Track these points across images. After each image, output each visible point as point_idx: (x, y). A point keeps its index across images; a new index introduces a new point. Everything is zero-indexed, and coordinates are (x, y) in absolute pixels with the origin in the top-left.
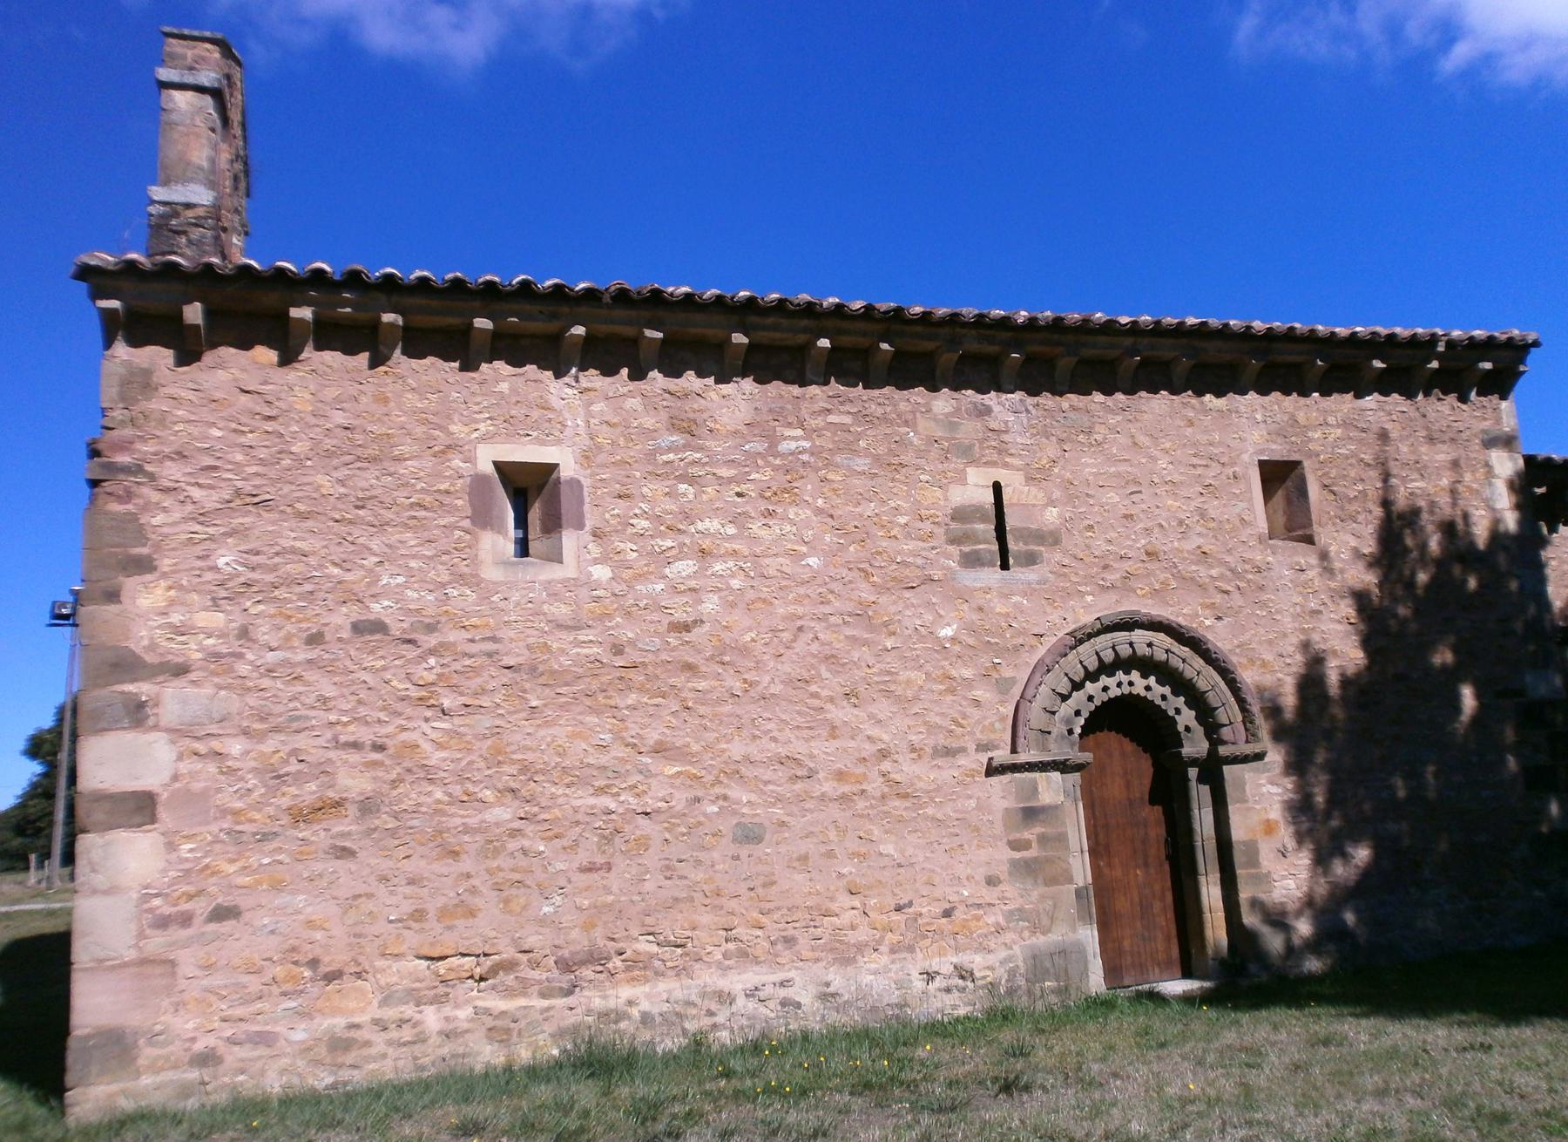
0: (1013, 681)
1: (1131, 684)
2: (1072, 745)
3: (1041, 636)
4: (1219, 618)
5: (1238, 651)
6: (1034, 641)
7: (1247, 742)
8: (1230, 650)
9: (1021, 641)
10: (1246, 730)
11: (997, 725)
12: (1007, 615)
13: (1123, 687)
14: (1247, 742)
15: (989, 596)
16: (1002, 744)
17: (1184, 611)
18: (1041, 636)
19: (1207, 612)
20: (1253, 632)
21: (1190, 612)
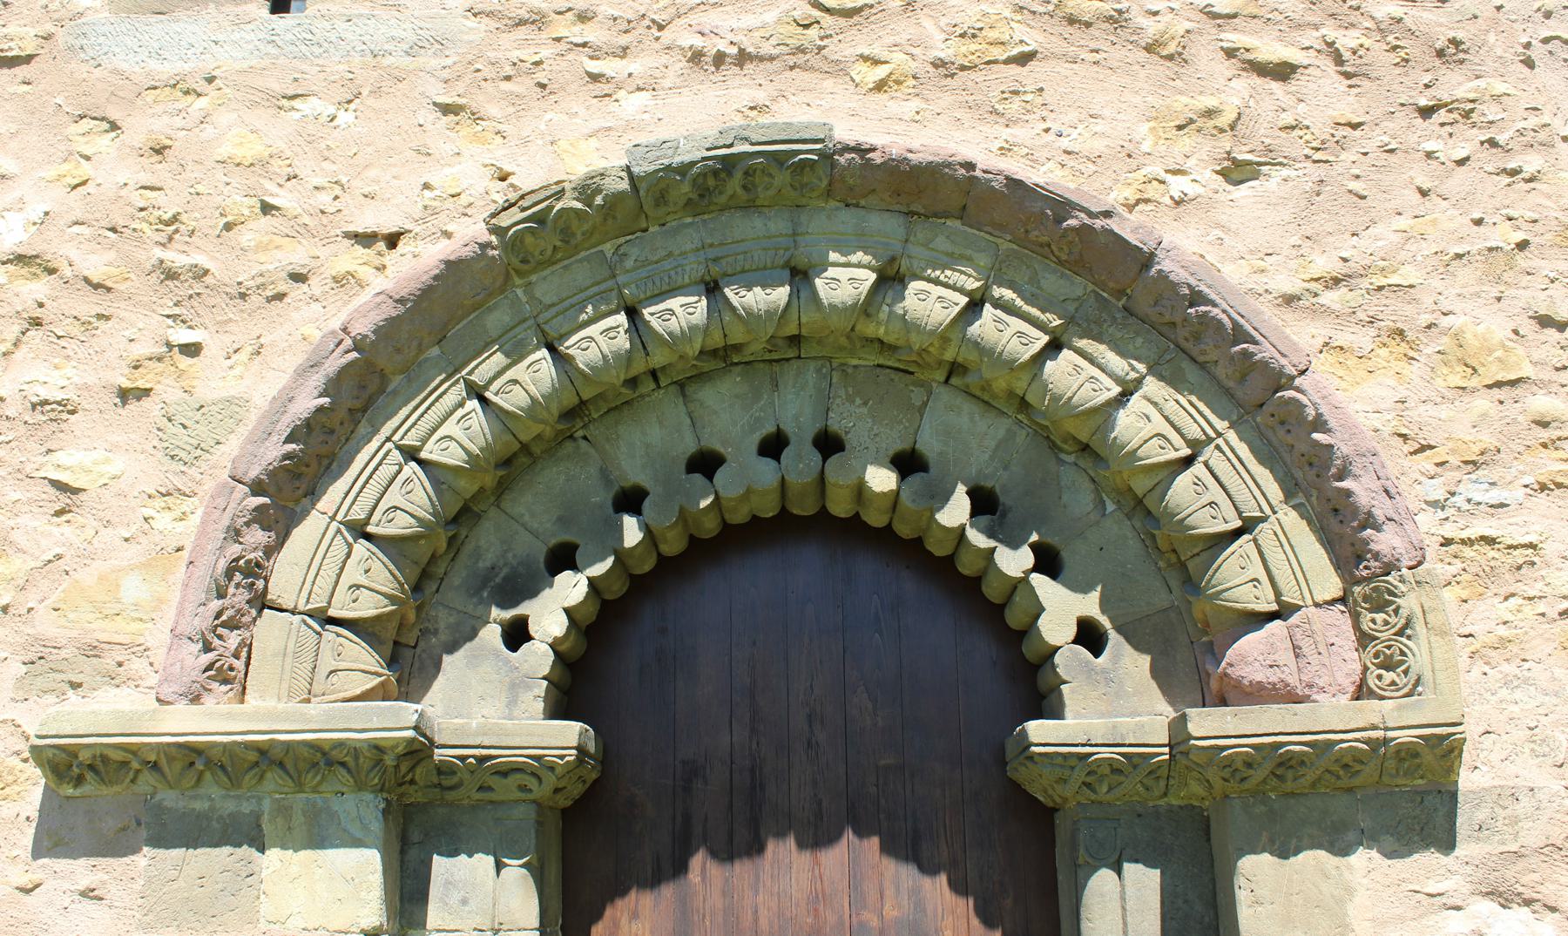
0: (233, 405)
1: (828, 444)
2: (515, 688)
3: (392, 241)
4: (1237, 172)
5: (1331, 298)
6: (353, 259)
7: (1362, 691)
8: (1289, 300)
9: (297, 255)
10: (1364, 639)
11: (134, 589)
12: (259, 165)
13: (787, 454)
14: (1362, 691)
15: (202, 102)
16: (137, 665)
17: (1065, 143)
18: (392, 241)
19: (1187, 141)
20: (1403, 223)
21: (1098, 146)
